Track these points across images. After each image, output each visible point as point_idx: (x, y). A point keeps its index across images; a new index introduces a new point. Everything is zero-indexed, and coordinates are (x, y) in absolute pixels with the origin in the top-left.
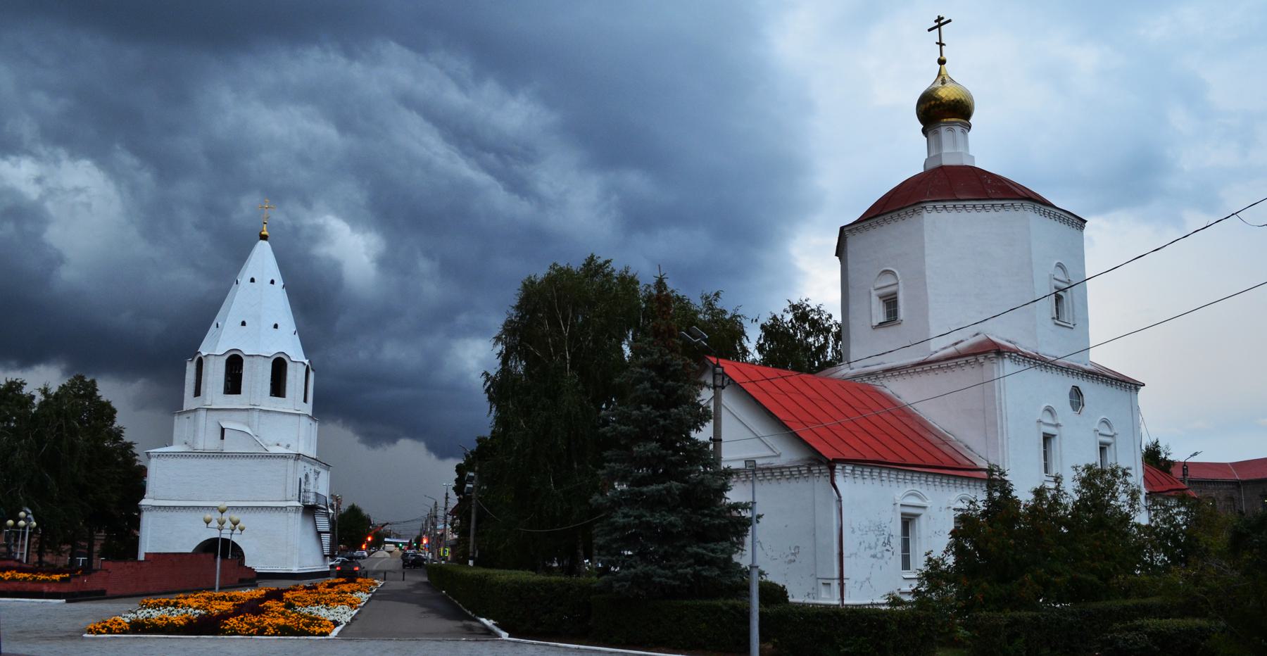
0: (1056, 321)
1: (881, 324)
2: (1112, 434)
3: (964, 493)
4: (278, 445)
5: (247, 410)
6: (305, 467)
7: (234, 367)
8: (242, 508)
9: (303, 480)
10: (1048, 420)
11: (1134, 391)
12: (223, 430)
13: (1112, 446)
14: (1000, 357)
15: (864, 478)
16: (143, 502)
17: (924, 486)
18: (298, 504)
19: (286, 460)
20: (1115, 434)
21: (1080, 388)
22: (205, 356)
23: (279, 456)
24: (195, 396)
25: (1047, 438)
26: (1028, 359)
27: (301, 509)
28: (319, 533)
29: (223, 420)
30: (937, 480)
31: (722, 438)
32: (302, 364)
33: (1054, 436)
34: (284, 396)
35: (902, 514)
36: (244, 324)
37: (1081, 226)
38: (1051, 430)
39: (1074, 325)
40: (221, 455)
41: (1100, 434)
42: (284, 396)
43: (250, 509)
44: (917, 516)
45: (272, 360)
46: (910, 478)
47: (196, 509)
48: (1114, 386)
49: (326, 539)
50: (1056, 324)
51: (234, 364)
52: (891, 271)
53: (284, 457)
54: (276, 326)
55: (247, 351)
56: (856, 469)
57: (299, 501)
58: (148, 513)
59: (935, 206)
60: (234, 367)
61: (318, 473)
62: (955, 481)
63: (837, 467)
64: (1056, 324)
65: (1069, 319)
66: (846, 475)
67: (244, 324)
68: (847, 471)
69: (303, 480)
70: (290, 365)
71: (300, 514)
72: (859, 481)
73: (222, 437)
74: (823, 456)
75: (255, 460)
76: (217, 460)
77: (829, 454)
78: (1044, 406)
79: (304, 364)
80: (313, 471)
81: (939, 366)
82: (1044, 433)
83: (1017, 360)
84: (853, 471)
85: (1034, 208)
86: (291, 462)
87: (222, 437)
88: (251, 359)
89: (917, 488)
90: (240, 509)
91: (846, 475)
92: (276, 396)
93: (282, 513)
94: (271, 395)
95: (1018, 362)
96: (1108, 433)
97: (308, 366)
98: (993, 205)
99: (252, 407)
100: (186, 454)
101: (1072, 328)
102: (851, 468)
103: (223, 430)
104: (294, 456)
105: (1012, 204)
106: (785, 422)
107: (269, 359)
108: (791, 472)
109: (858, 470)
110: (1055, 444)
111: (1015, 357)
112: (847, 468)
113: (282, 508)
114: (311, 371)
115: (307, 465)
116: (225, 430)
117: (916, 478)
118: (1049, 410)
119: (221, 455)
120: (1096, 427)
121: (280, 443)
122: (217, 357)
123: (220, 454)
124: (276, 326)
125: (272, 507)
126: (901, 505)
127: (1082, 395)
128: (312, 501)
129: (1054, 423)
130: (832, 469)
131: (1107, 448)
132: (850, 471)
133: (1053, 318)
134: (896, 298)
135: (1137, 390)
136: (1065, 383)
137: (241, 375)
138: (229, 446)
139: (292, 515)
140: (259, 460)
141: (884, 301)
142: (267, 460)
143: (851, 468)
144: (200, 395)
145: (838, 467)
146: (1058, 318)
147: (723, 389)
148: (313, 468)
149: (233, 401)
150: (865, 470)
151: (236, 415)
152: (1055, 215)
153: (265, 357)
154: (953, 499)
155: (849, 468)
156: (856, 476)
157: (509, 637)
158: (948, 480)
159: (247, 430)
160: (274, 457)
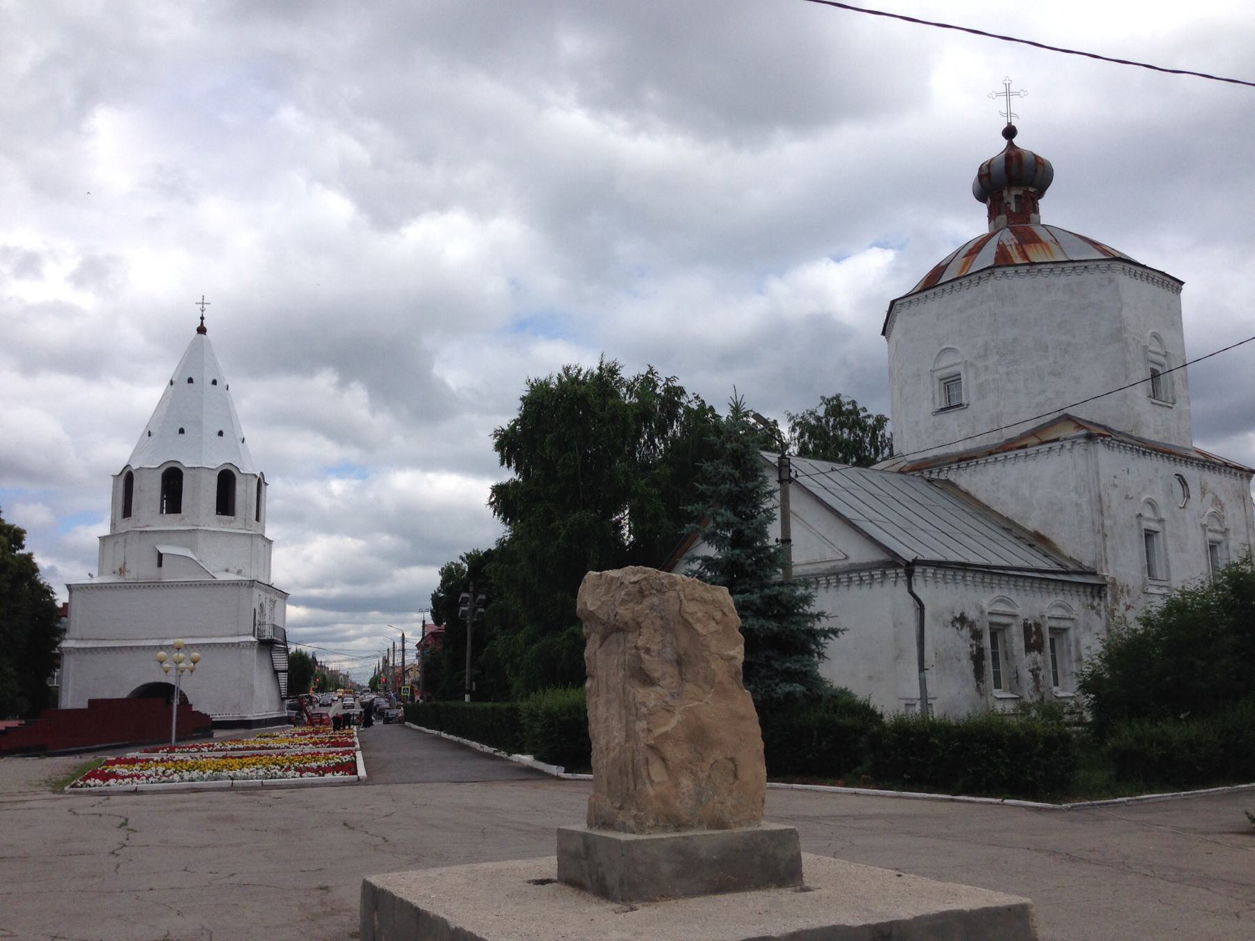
0: (1155, 401)
1: (943, 409)
2: (1223, 530)
3: (1059, 599)
4: (227, 571)
5: (189, 531)
6: (260, 595)
9: (258, 611)
10: (1148, 513)
11: (1245, 479)
13: (1224, 545)
14: (1091, 444)
15: (946, 583)
16: (64, 644)
17: (1014, 592)
18: (252, 639)
20: (1226, 529)
21: (1185, 477)
22: (137, 470)
24: (124, 517)
25: (1149, 535)
26: (1124, 444)
27: (256, 644)
28: (276, 672)
29: (157, 544)
30: (1027, 584)
31: (792, 538)
32: (253, 477)
33: (1157, 532)
34: (232, 514)
35: (991, 624)
36: (182, 431)
37: (1177, 288)
38: (1154, 526)
39: (1173, 404)
40: (157, 585)
41: (1210, 530)
42: (232, 514)
44: (1007, 626)
46: (997, 582)
48: (1223, 475)
49: (283, 678)
50: (1153, 403)
51: (172, 481)
52: (954, 349)
53: (237, 584)
54: (221, 434)
55: (186, 462)
56: (938, 572)
57: (254, 636)
59: (1004, 272)
61: (275, 602)
62: (1047, 585)
63: (917, 570)
64: (1153, 403)
65: (1167, 398)
66: (927, 579)
67: (182, 431)
68: (928, 575)
69: (258, 611)
70: (238, 477)
71: (256, 650)
72: (941, 585)
73: (160, 565)
74: (901, 558)
77: (909, 555)
78: (1145, 497)
80: (268, 600)
81: (1016, 455)
82: (1145, 529)
83: (1111, 445)
84: (934, 574)
85: (1123, 269)
87: (160, 565)
88: (192, 472)
89: (1005, 593)
91: (927, 579)
92: (223, 514)
93: (233, 648)
94: (217, 514)
95: (1113, 447)
96: (1217, 527)
97: (259, 479)
98: (1074, 268)
99: (195, 528)
101: (1171, 408)
102: (933, 571)
103: (160, 556)
104: (248, 583)
105: (1098, 266)
106: (853, 521)
107: (214, 472)
108: (861, 577)
109: (940, 573)
110: (1158, 542)
111: (1109, 441)
112: (928, 570)
113: (233, 644)
114: (263, 484)
115: (262, 593)
116: (163, 555)
117: (1005, 582)
118: (1151, 504)
119: (157, 585)
120: (1205, 521)
121: (230, 569)
124: (221, 434)
126: (989, 613)
127: (1187, 485)
128: (268, 634)
129: (1156, 518)
130: (910, 573)
131: (1218, 546)
132: (931, 575)
133: (1150, 396)
134: (960, 379)
135: (1249, 478)
136: (1164, 469)
138: (168, 574)
139: (247, 652)
141: (945, 384)
143: (933, 571)
145: (918, 569)
146: (1154, 398)
147: (790, 483)
148: (268, 596)
149: (171, 522)
150: (948, 573)
152: (1147, 277)
153: (209, 469)
154: (1047, 606)
155: (930, 571)
156: (938, 580)
157: (565, 772)
158: (1040, 584)
159: (191, 555)
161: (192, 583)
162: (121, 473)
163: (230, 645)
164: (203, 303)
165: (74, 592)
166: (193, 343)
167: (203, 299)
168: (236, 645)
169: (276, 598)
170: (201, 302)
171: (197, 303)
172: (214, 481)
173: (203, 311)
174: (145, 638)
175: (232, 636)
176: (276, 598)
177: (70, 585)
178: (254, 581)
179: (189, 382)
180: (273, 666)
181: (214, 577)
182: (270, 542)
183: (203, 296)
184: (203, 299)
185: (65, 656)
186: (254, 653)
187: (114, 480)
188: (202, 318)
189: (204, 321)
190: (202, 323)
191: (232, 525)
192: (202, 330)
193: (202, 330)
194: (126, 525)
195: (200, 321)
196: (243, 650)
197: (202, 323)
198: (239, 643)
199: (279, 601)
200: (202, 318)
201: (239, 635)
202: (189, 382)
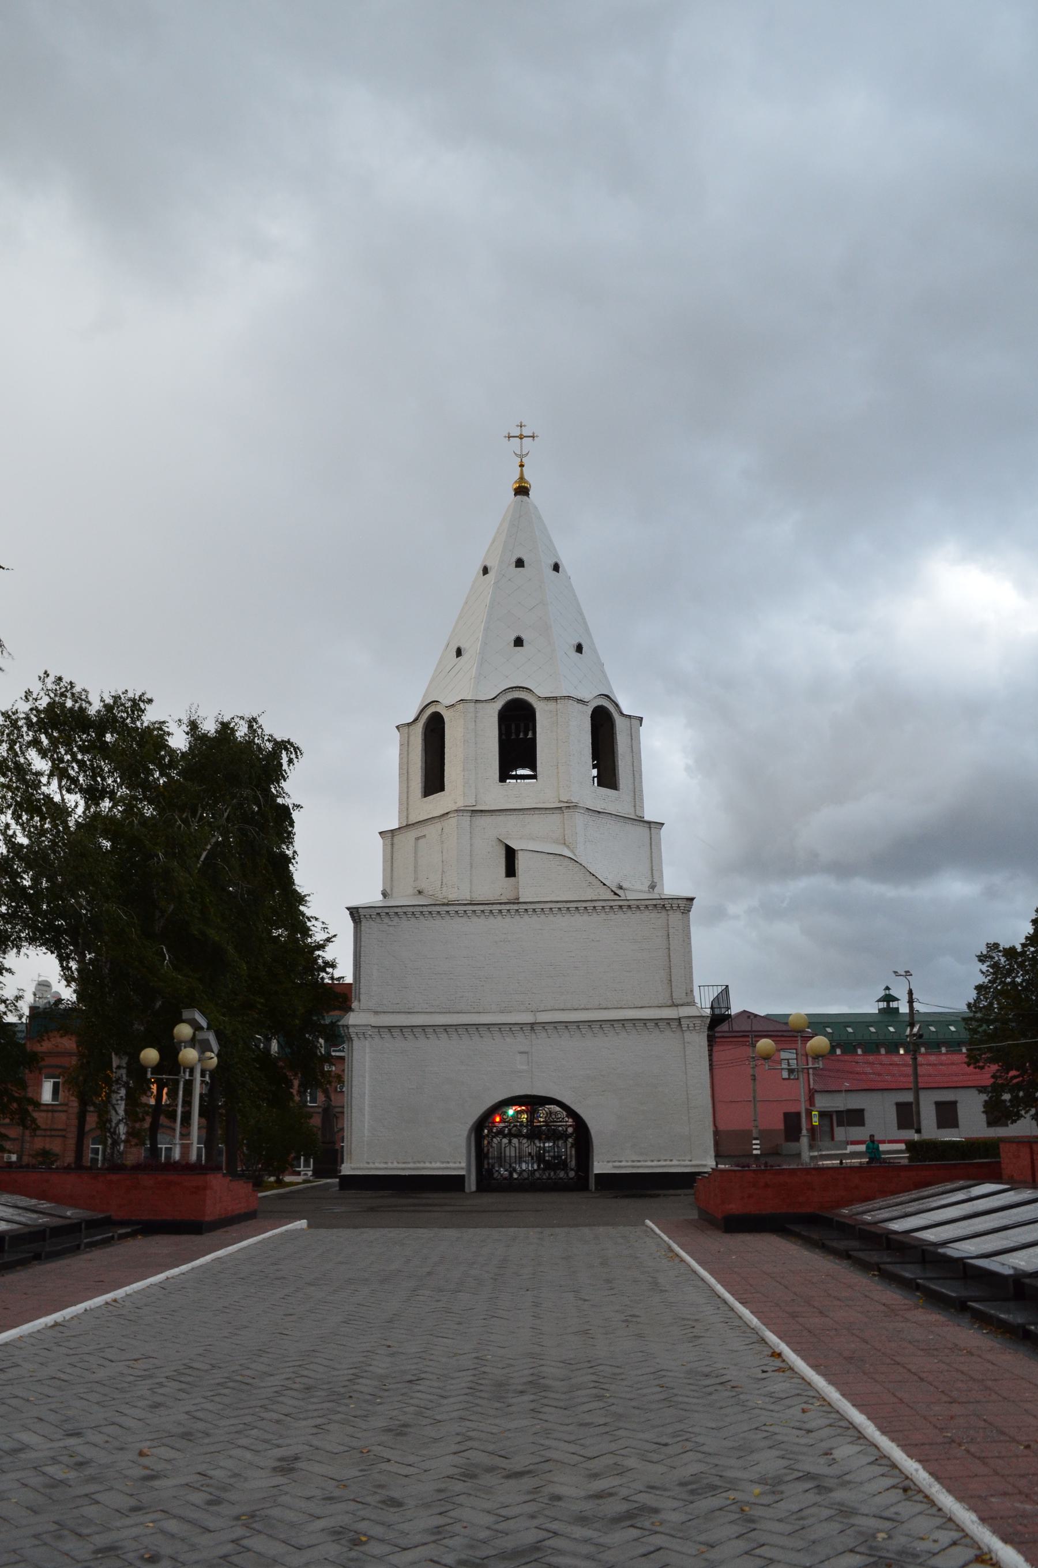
8: (578, 1024)
12: (510, 854)
16: (353, 1019)
19: (664, 913)
23: (647, 907)
36: (519, 642)
67: (519, 642)
73: (511, 871)
75: (595, 917)
87: (511, 871)
88: (551, 705)
100: (438, 909)
113: (668, 1021)
119: (514, 906)
122: (479, 705)
123: (516, 907)
125: (645, 1021)
137: (533, 742)
142: (620, 916)
144: (442, 788)
160: (638, 907)
161: (579, 905)
162: (416, 719)
165: (364, 923)
168: (674, 1024)
177: (357, 908)
179: (517, 566)
181: (616, 894)
185: (356, 1044)
186: (699, 1041)
192: (522, 490)
193: (522, 490)
194: (439, 803)
196: (687, 1035)
198: (679, 1019)
201: (674, 1005)
202: (517, 566)
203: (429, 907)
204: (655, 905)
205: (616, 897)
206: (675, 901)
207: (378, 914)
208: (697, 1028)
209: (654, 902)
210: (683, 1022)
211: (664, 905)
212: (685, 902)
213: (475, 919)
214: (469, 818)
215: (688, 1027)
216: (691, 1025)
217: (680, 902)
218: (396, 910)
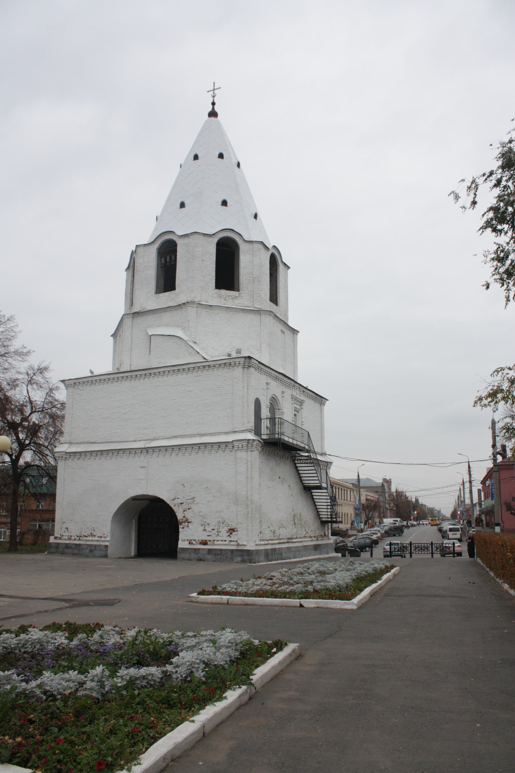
6: (267, 384)
7: (168, 258)
8: (173, 447)
18: (251, 436)
23: (220, 365)
34: (238, 290)
42: (238, 290)
43: (183, 449)
45: (215, 240)
47: (116, 453)
54: (224, 203)
58: (63, 462)
60: (168, 258)
61: (301, 403)
67: (182, 205)
76: (142, 381)
79: (267, 248)
86: (238, 371)
88: (186, 240)
90: (170, 450)
100: (104, 377)
107: (211, 239)
113: (226, 443)
139: (242, 455)
140: (195, 373)
142: (206, 373)
151: (167, 317)
153: (204, 235)
159: (179, 333)
160: (214, 366)
163: (223, 446)
164: (214, 90)
166: (205, 129)
167: (214, 86)
169: (302, 398)
170: (212, 89)
171: (208, 92)
172: (213, 250)
173: (214, 97)
174: (133, 439)
175: (227, 433)
176: (302, 398)
178: (250, 358)
180: (301, 481)
181: (205, 358)
182: (294, 332)
183: (214, 83)
184: (214, 86)
187: (127, 274)
188: (213, 104)
189: (215, 106)
190: (213, 108)
191: (237, 302)
192: (213, 114)
193: (213, 114)
195: (212, 106)
196: (239, 452)
197: (213, 108)
198: (233, 441)
199: (309, 404)
200: (213, 104)
203: (100, 377)
204: (225, 364)
205: (205, 360)
206: (237, 360)
207: (75, 383)
208: (244, 448)
209: (224, 362)
210: (236, 444)
211: (230, 363)
212: (243, 360)
213: (124, 382)
214: (131, 319)
215: (238, 448)
216: (240, 446)
217: (240, 360)
218: (84, 380)
